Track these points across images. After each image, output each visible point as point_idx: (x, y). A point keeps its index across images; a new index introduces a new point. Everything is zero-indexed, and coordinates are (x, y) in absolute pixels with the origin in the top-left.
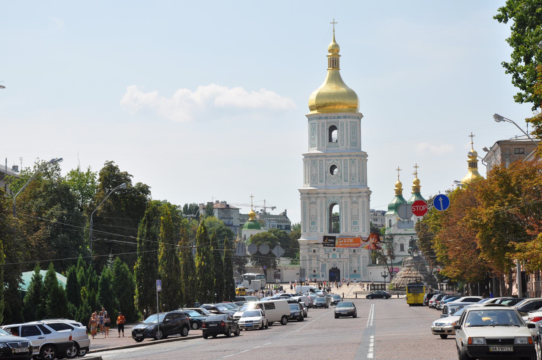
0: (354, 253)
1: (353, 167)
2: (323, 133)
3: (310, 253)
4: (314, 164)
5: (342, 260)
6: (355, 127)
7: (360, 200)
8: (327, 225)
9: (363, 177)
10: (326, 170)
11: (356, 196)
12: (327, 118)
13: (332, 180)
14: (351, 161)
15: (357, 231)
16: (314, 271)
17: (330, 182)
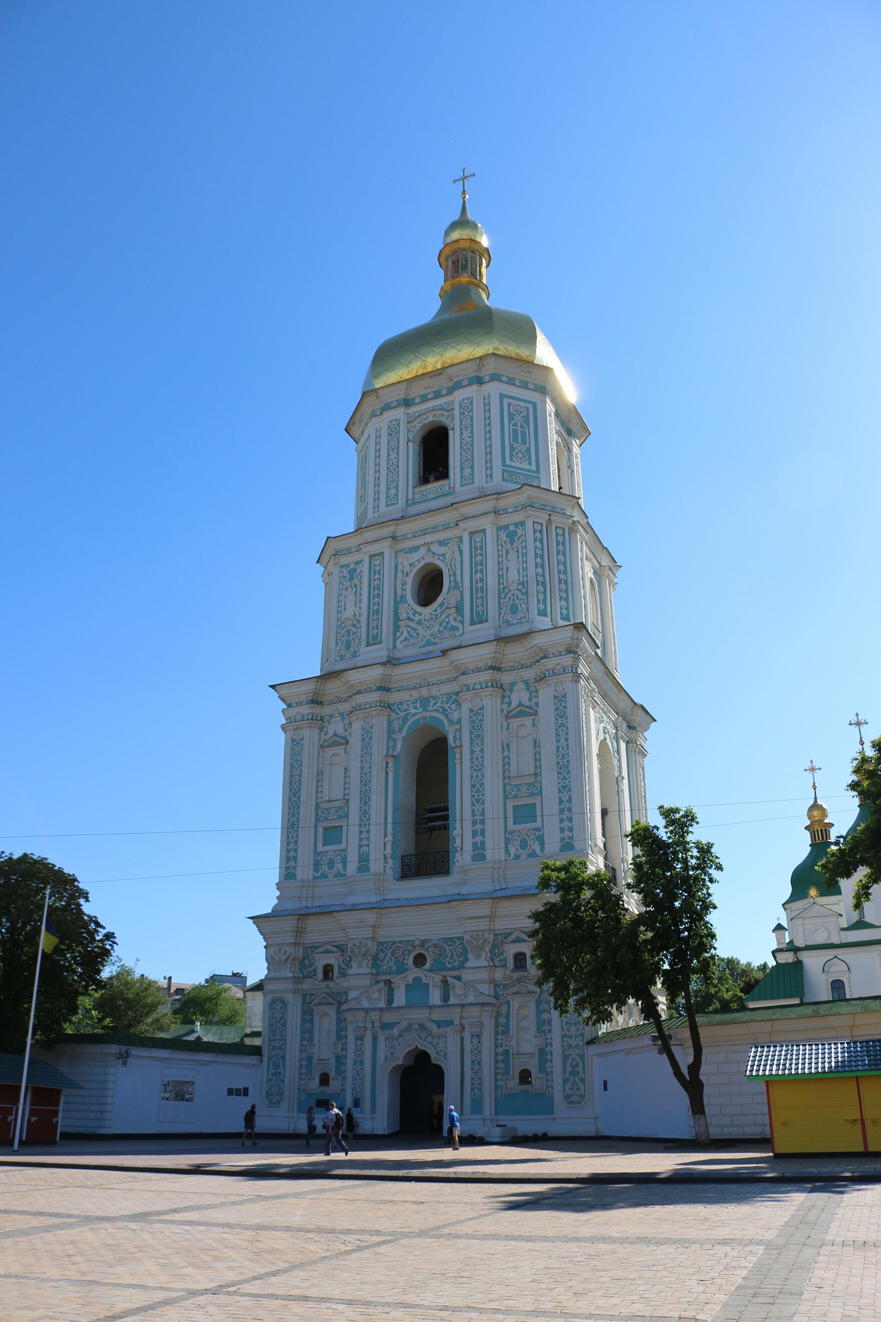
0: (516, 975)
1: (512, 556)
2: (393, 456)
3: (307, 985)
4: (351, 580)
5: (455, 1015)
6: (526, 419)
7: (546, 694)
8: (389, 838)
9: (567, 599)
10: (399, 594)
11: (526, 682)
12: (407, 403)
13: (420, 630)
14: (503, 537)
15: (533, 855)
16: (325, 1080)
17: (412, 641)
